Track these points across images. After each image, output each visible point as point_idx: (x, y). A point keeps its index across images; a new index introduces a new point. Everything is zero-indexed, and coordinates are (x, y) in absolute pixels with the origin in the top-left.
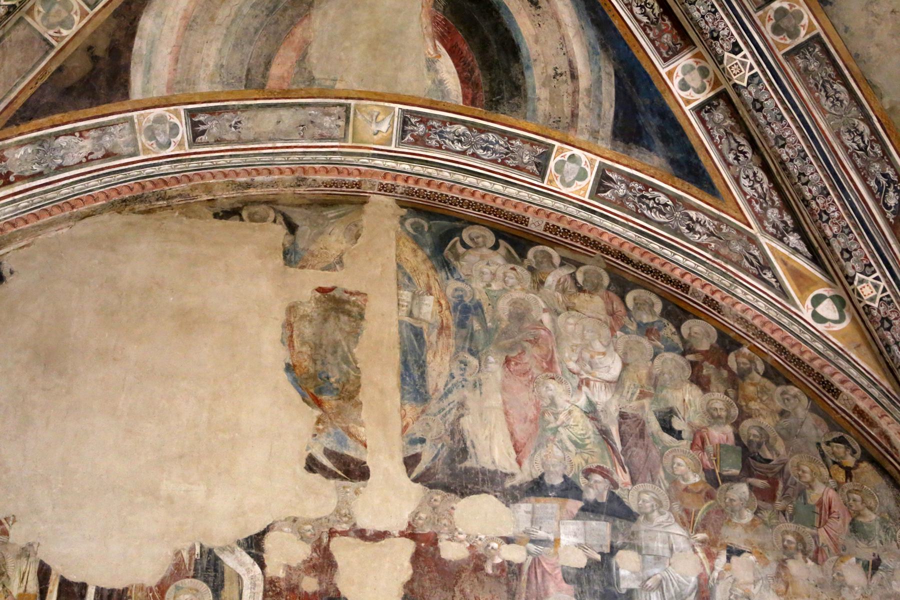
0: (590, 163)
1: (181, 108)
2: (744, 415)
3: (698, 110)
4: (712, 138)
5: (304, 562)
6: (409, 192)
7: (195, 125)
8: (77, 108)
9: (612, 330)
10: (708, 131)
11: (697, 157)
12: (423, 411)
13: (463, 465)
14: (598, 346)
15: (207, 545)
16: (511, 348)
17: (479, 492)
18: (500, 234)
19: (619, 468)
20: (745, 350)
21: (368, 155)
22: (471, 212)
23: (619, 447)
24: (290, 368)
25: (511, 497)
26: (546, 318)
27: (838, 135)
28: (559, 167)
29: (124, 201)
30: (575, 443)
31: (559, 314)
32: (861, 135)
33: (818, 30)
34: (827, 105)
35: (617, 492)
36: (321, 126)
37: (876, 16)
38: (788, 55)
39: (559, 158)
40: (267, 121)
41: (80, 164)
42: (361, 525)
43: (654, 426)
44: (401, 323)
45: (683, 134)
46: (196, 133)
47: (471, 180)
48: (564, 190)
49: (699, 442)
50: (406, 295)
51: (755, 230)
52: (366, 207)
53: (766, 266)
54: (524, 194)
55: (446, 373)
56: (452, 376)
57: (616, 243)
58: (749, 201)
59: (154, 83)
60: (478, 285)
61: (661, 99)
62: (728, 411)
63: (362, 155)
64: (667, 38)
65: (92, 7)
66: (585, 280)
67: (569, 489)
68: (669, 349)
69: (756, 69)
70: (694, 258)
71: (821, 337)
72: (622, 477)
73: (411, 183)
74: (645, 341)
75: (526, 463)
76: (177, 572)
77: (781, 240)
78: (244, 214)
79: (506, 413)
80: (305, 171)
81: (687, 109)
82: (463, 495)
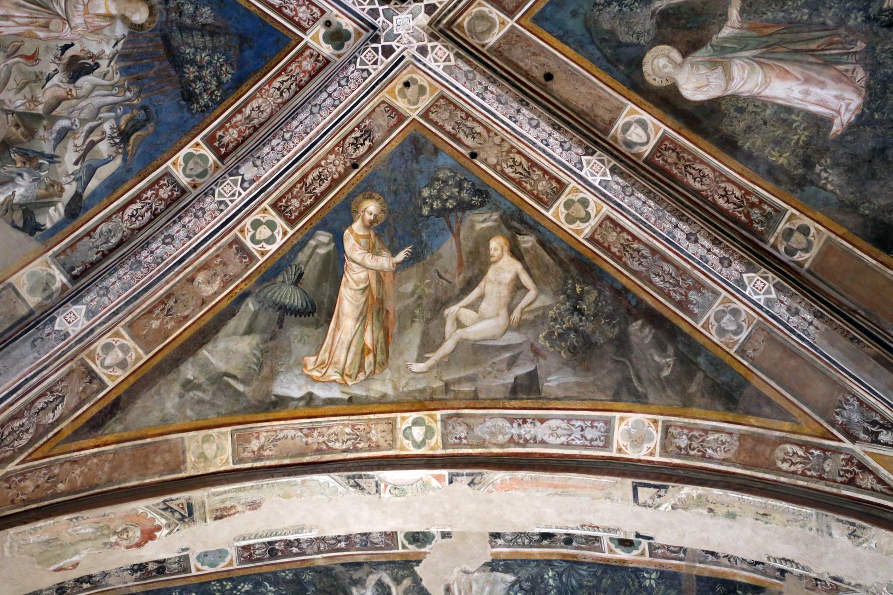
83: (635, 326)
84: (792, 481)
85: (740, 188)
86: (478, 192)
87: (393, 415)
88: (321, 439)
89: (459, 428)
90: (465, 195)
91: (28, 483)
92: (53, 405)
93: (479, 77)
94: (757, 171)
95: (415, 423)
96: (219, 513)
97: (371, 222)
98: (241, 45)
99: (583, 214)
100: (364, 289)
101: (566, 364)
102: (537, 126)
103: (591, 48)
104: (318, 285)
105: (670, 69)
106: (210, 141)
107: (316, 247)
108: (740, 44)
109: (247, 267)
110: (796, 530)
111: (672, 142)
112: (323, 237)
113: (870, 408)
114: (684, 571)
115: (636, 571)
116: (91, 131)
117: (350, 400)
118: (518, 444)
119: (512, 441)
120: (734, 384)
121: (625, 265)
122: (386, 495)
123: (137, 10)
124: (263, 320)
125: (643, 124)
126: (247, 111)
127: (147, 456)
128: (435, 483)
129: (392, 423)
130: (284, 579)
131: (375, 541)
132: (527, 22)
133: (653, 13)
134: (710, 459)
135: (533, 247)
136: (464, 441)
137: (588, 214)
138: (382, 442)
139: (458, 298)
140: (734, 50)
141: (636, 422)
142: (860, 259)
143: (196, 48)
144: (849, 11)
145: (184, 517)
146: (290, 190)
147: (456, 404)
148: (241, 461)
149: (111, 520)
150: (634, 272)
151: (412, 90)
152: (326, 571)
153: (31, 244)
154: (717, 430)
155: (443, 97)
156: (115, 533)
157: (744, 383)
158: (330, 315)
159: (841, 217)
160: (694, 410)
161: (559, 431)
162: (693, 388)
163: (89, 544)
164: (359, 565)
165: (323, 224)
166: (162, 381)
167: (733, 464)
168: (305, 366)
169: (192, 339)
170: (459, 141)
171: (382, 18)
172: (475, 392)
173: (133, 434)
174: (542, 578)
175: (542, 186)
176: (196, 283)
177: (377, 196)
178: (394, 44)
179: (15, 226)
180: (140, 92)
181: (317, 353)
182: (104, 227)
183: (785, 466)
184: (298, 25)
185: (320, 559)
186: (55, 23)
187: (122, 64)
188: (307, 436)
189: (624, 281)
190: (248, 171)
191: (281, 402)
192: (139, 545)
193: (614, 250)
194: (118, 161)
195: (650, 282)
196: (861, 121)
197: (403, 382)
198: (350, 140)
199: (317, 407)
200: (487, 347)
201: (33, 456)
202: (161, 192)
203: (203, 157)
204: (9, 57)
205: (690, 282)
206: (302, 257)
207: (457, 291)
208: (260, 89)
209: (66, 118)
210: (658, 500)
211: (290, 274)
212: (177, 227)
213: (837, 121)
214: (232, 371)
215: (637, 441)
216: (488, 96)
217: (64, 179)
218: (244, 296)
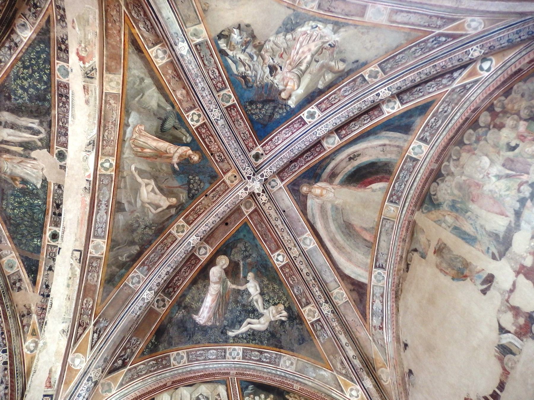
0: (416, 143)
1: (374, 269)
2: (518, 113)
3: (402, 104)
4: (413, 100)
5: (513, 317)
6: (415, 206)
7: (379, 267)
8: (366, 300)
9: (474, 154)
10: (410, 101)
11: (419, 106)
12: (479, 242)
13: (501, 239)
14: (478, 162)
15: (496, 345)
16: (469, 197)
17: (512, 239)
18: (434, 180)
19: (521, 177)
20: (495, 102)
21: (401, 215)
22: (426, 187)
23: (514, 173)
24: (453, 279)
25: (518, 227)
26: (464, 178)
27: (416, 57)
28: (415, 154)
29: (396, 297)
30: (507, 190)
31: (463, 172)
32: (416, 50)
33: (376, 65)
34: (404, 61)
35: (530, 182)
36: (388, 228)
37: (371, 47)
38: (385, 73)
39: (412, 154)
40: (383, 244)
41: (383, 305)
42: (508, 289)
43: (510, 154)
44: (451, 232)
45: (410, 110)
46: (382, 267)
47: (415, 184)
48: (424, 153)
49: (522, 137)
50: (443, 225)
51: (450, 89)
52: (417, 222)
53: (464, 86)
54: (423, 167)
55: (470, 226)
56: (471, 224)
57: (446, 140)
58: (438, 89)
59: (364, 275)
60: (447, 197)
61: (397, 116)
62: (514, 120)
63: (400, 217)
64: (376, 113)
65: (339, 286)
66: (456, 156)
67: (522, 201)
68: (486, 135)
69: (386, 88)
70: (457, 113)
71: (496, 71)
72: (525, 177)
73: (412, 205)
74: (482, 143)
75: (509, 214)
76: (501, 360)
77: (455, 79)
78: (409, 263)
79: (489, 211)
80: (401, 238)
81: (401, 108)
82: (511, 245)
83: (138, 248)
84: (80, 304)
85: (180, 285)
86: (193, 196)
87: (115, 156)
88: (110, 127)
89: (107, 181)
90: (193, 191)
91: (115, 13)
92: (146, 27)
93: (233, 206)
94: (185, 291)
95: (111, 165)
96: (86, 88)
97: (191, 157)
98: (263, 124)
99: (179, 231)
100: (166, 151)
101: (127, 222)
102: (213, 223)
103: (233, 239)
104: (171, 135)
105: (221, 264)
106: (234, 106)
107: (186, 136)
108: (225, 287)
109: (184, 109)
110: (64, 310)
111: (198, 263)
112: (189, 139)
113: (105, 330)
114: (41, 256)
115: (41, 238)
116: (250, 67)
117: (124, 141)
118: (98, 203)
119: (99, 201)
120: (115, 283)
121: (159, 244)
122: (84, 154)
123: (286, 95)
124: (162, 112)
125: (205, 254)
126: (241, 121)
127: (115, 59)
128: (87, 174)
129: (112, 155)
130: (47, 95)
131: (61, 138)
132: (245, 220)
133: (239, 261)
134: (88, 274)
135: (170, 213)
136: (101, 183)
137: (179, 233)
138: (105, 151)
139: (157, 185)
140: (223, 285)
141: (103, 248)
142: (154, 324)
143: (267, 110)
144: (228, 321)
145: (87, 74)
146: (209, 130)
147: (117, 180)
148: (106, 95)
149: (92, 47)
150: (156, 248)
151: (233, 178)
152: (48, 112)
153: (214, 34)
154: (98, 276)
155: (228, 188)
156: (86, 46)
157: (114, 286)
158: (159, 138)
159: (167, 318)
160: (106, 268)
161: (101, 219)
162: (114, 268)
163: (83, 36)
164: (50, 127)
165: (193, 140)
166: (146, 70)
167: (86, 283)
168: (141, 125)
169: (161, 84)
170: (212, 192)
171: (260, 178)
172: (120, 188)
173: (126, 56)
174: (38, 199)
175: (191, 218)
176: (182, 89)
177: (200, 160)
178: (251, 180)
179: (222, 31)
180: (258, 87)
181: (145, 130)
182: (212, 60)
183: (85, 301)
184: (264, 145)
185: (55, 112)
186: (290, 67)
187: (269, 84)
188: (112, 122)
189: (154, 244)
190: (221, 122)
191: (128, 114)
192: (78, 53)
193: (165, 241)
194: (235, 72)
195: (152, 253)
196: (195, 324)
197: (128, 161)
198: (221, 154)
199: (123, 127)
200: (137, 194)
201: (126, 17)
202: (220, 84)
203: (229, 102)
204: (284, 49)
205: (151, 266)
206: (183, 130)
207: (159, 185)
208: (247, 127)
209: (256, 61)
210: (74, 259)
211: (178, 125)
212: (207, 93)
213: (197, 317)
214: (144, 97)
215: (96, 248)
216: (226, 208)
217: (235, 52)
218: (173, 106)
